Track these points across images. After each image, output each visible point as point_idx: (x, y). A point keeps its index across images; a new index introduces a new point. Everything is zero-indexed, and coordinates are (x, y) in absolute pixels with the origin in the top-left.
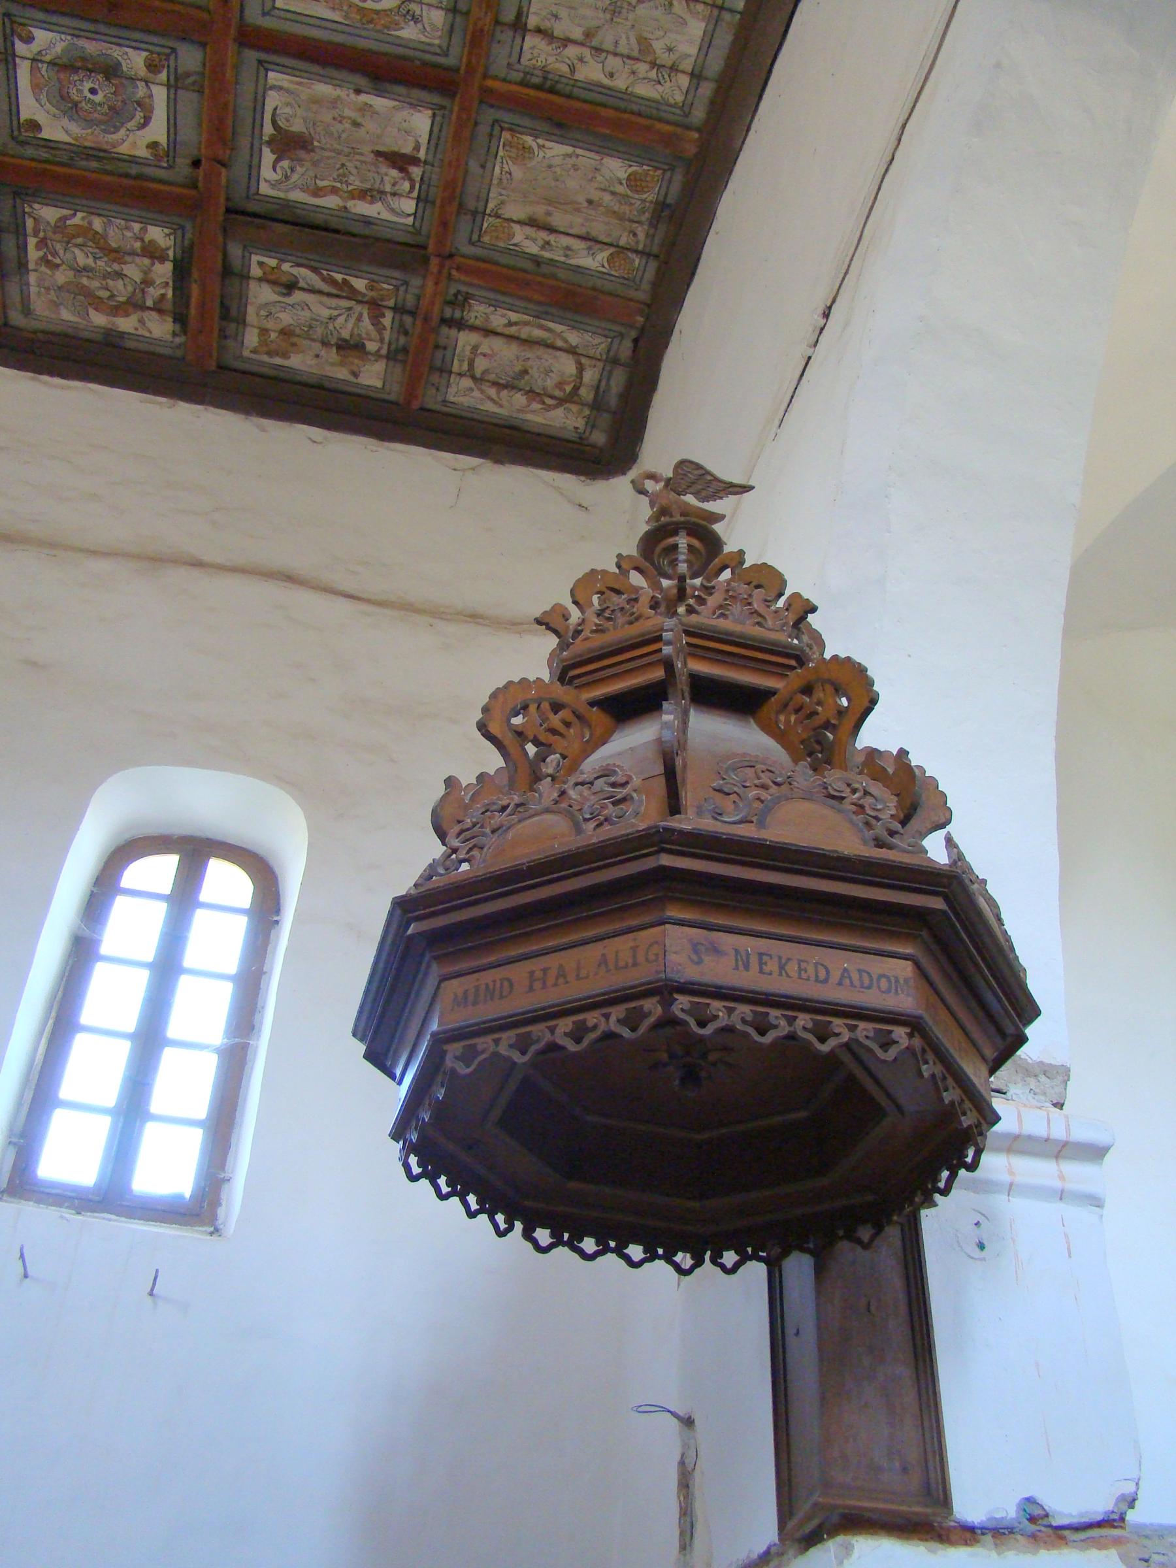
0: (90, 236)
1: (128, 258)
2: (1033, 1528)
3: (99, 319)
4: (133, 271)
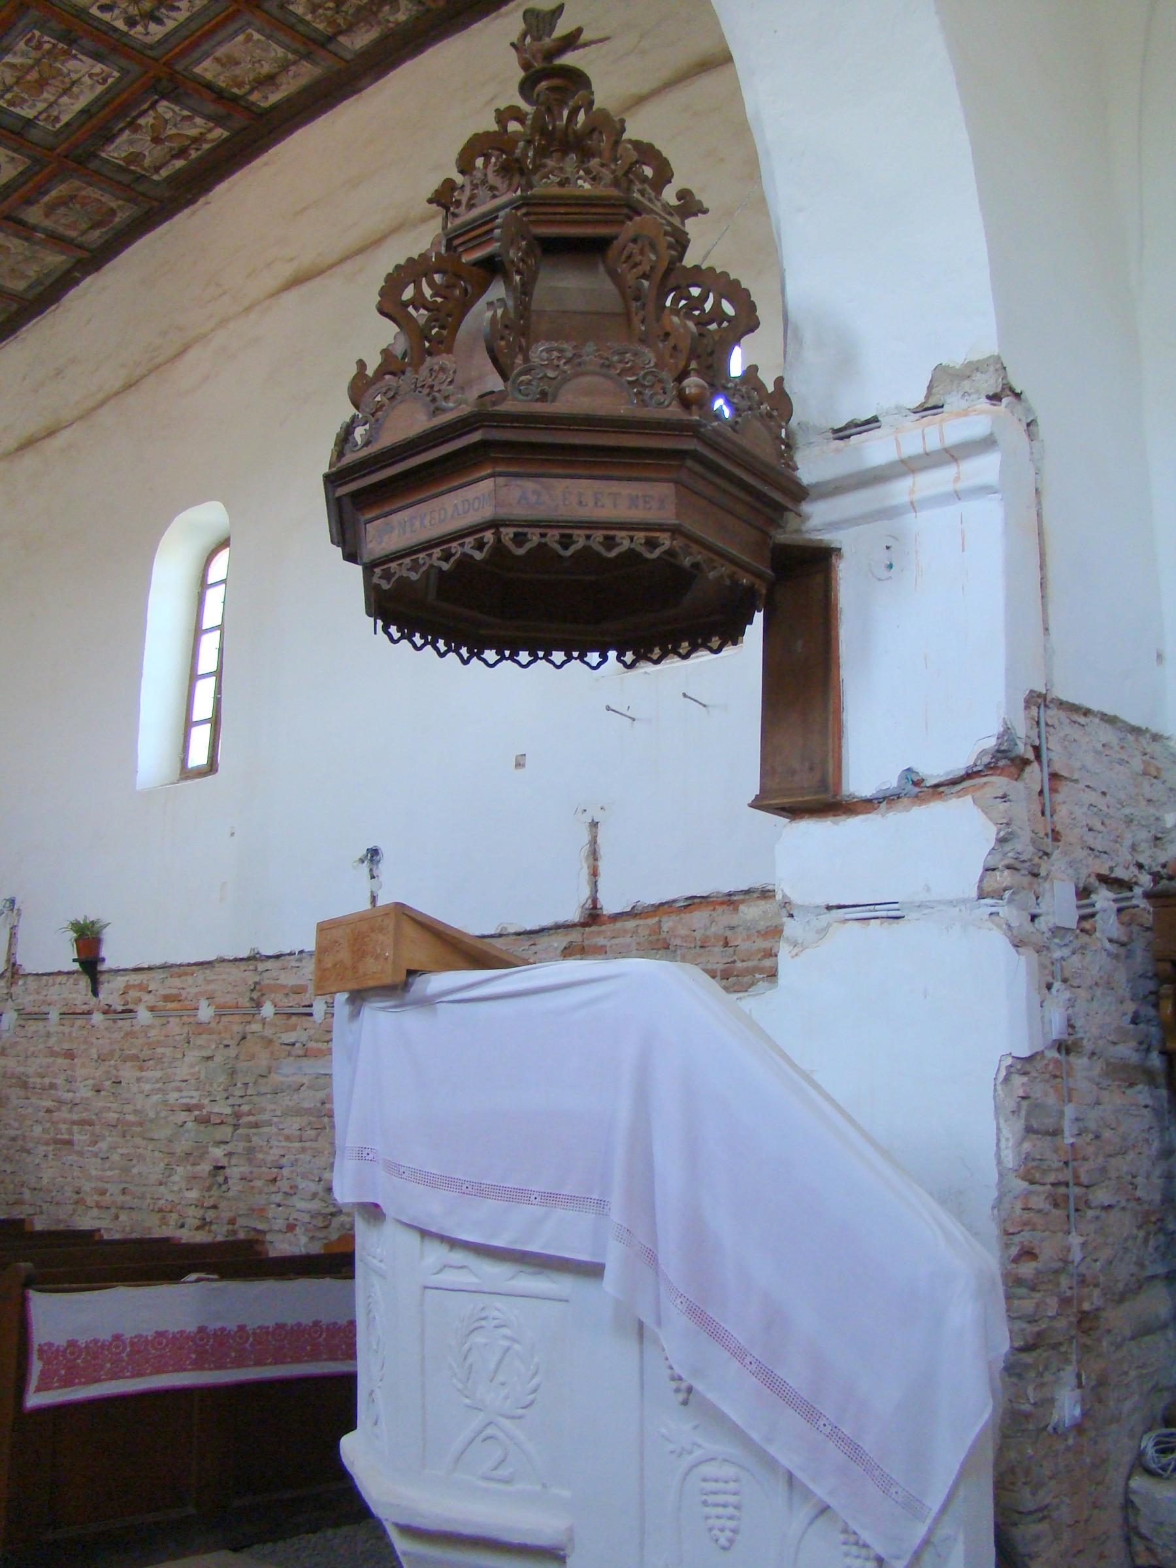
2: (917, 790)
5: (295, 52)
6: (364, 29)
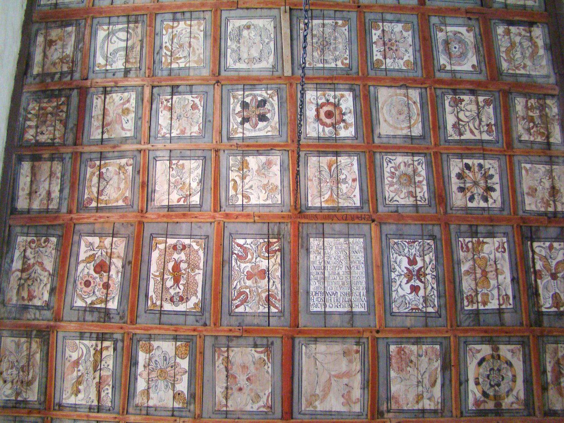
0: (508, 52)
1: (513, 40)
3: (541, 52)
4: (518, 39)
5: (546, 163)
6: (552, 128)
